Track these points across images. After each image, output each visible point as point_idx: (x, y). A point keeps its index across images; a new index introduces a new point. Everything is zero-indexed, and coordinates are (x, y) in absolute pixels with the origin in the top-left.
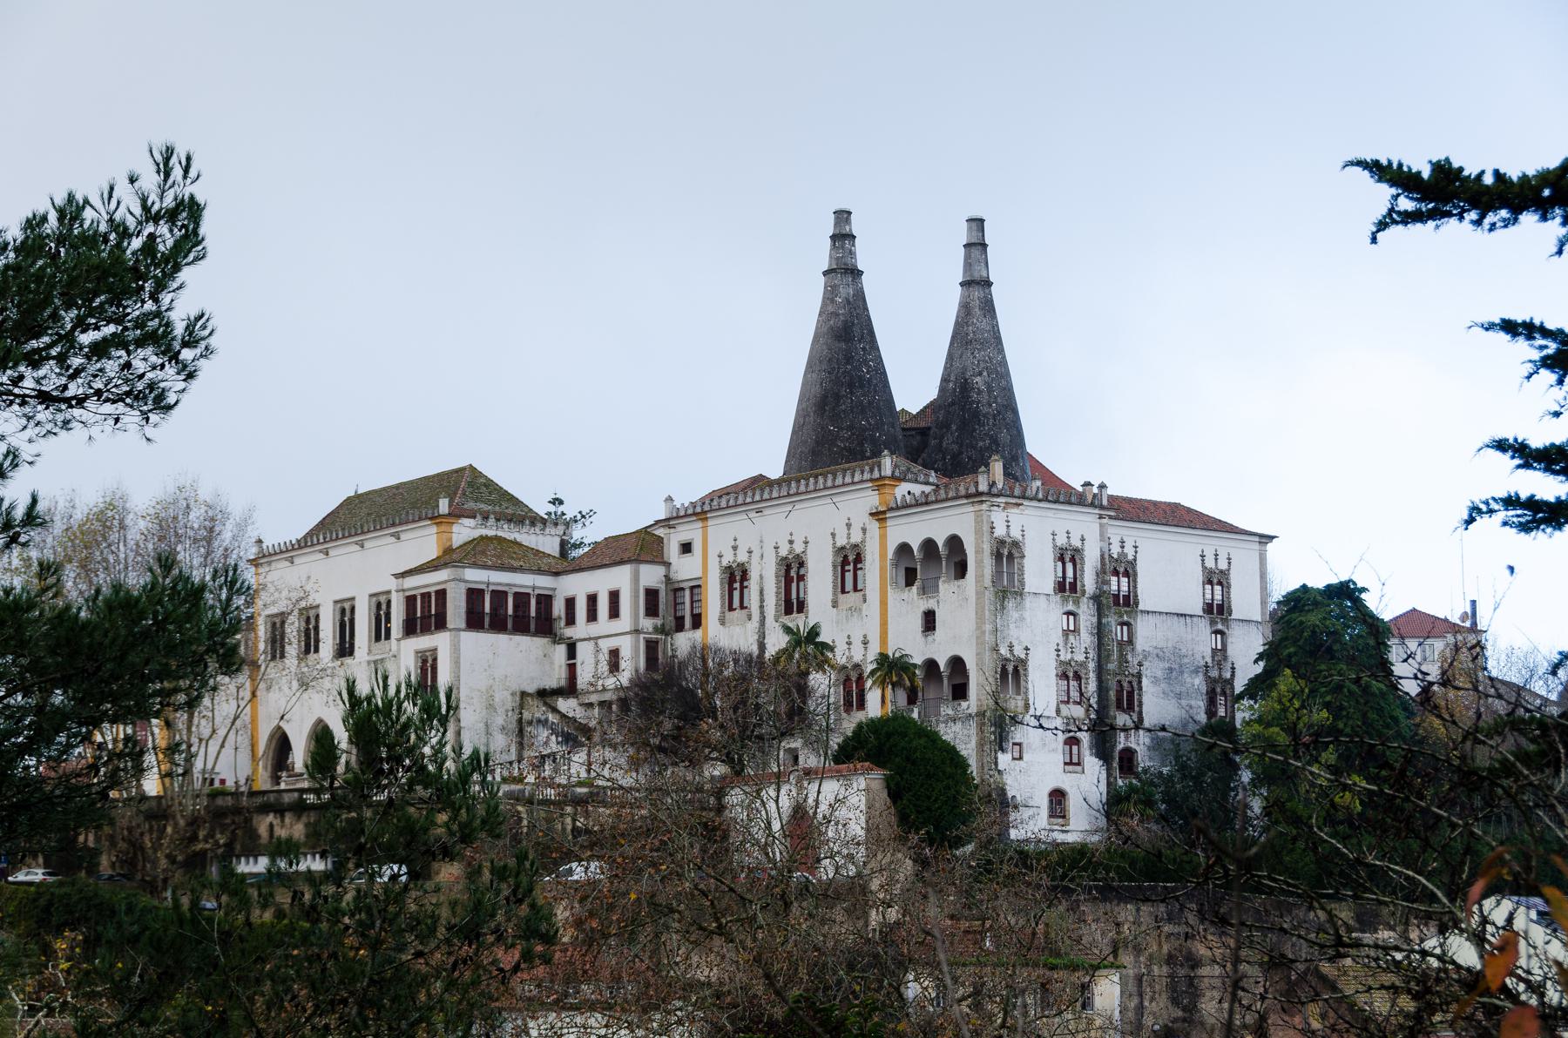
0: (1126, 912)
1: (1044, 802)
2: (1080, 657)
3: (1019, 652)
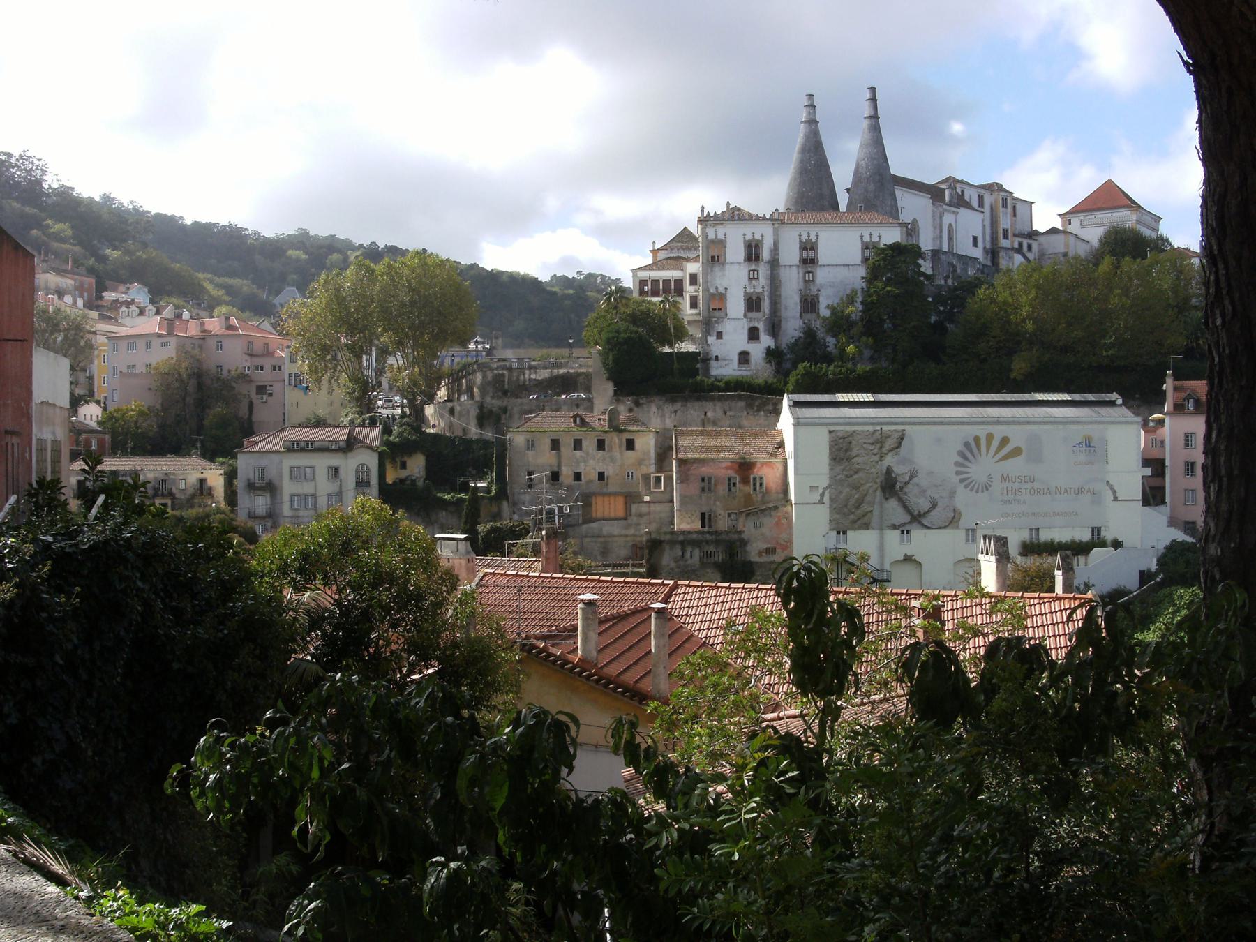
0: (709, 406)
1: (736, 358)
2: (759, 290)
3: (721, 290)
